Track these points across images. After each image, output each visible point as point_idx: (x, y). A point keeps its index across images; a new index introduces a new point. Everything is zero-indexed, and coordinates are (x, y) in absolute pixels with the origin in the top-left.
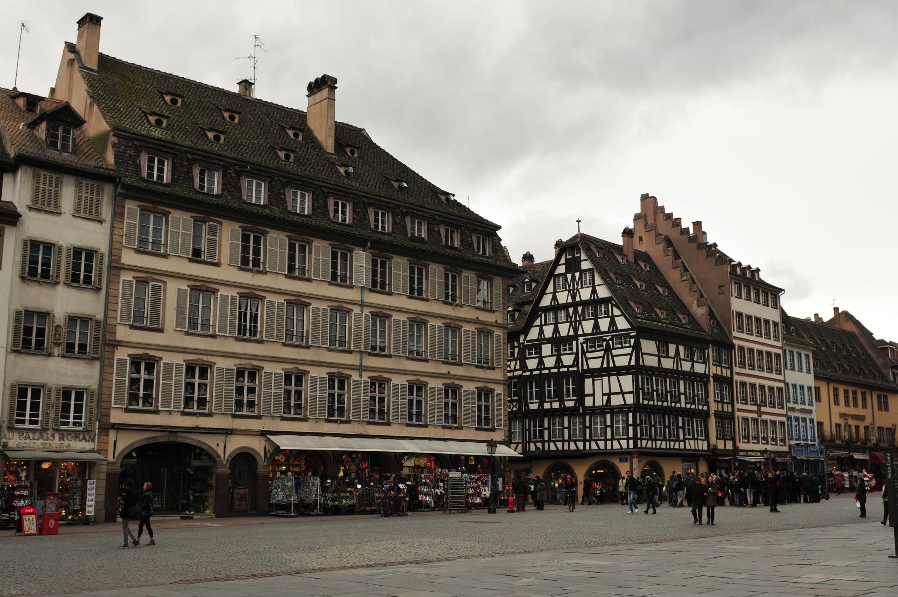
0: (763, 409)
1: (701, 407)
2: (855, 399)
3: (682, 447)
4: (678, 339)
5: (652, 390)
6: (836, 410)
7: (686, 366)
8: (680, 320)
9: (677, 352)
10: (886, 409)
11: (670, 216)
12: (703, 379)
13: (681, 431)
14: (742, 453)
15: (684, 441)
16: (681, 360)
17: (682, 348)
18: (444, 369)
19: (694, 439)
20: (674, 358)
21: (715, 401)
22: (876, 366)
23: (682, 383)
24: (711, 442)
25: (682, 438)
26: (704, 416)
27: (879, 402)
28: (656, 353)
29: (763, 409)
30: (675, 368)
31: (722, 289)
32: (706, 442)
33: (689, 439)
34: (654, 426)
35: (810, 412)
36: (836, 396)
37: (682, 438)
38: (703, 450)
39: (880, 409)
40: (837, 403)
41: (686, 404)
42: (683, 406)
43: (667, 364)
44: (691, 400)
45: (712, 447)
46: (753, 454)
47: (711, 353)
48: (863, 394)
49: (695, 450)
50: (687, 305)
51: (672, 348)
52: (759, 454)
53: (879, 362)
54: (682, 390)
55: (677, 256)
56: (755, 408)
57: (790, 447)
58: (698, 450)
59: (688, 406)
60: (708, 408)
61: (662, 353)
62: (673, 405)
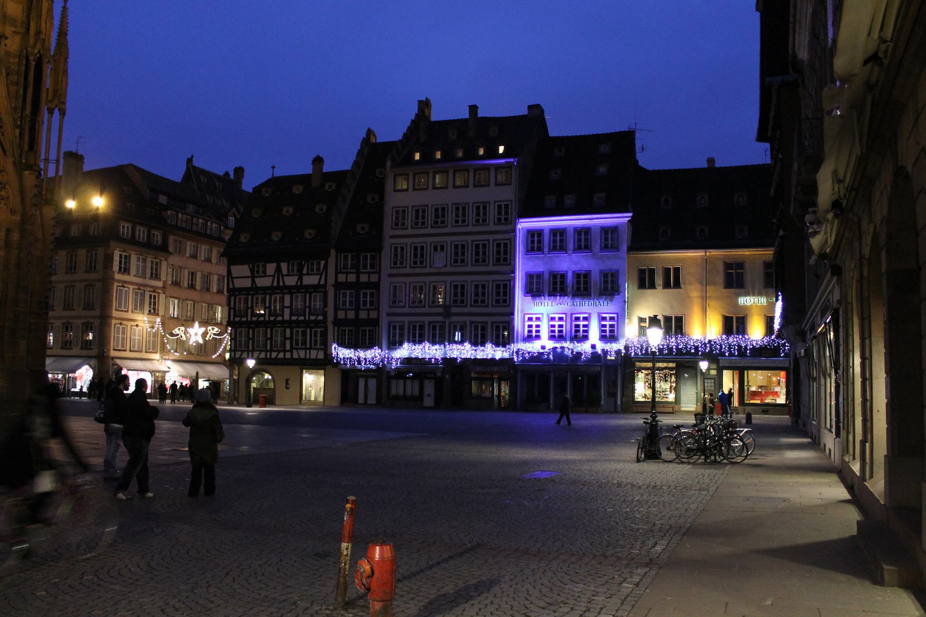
3: (288, 355)
7: (291, 281)
9: (278, 269)
15: (291, 351)
16: (283, 276)
17: (284, 266)
18: (84, 313)
20: (274, 276)
28: (250, 275)
30: (275, 284)
33: (297, 349)
34: (267, 339)
38: (316, 359)
42: (287, 317)
49: (305, 359)
59: (294, 318)
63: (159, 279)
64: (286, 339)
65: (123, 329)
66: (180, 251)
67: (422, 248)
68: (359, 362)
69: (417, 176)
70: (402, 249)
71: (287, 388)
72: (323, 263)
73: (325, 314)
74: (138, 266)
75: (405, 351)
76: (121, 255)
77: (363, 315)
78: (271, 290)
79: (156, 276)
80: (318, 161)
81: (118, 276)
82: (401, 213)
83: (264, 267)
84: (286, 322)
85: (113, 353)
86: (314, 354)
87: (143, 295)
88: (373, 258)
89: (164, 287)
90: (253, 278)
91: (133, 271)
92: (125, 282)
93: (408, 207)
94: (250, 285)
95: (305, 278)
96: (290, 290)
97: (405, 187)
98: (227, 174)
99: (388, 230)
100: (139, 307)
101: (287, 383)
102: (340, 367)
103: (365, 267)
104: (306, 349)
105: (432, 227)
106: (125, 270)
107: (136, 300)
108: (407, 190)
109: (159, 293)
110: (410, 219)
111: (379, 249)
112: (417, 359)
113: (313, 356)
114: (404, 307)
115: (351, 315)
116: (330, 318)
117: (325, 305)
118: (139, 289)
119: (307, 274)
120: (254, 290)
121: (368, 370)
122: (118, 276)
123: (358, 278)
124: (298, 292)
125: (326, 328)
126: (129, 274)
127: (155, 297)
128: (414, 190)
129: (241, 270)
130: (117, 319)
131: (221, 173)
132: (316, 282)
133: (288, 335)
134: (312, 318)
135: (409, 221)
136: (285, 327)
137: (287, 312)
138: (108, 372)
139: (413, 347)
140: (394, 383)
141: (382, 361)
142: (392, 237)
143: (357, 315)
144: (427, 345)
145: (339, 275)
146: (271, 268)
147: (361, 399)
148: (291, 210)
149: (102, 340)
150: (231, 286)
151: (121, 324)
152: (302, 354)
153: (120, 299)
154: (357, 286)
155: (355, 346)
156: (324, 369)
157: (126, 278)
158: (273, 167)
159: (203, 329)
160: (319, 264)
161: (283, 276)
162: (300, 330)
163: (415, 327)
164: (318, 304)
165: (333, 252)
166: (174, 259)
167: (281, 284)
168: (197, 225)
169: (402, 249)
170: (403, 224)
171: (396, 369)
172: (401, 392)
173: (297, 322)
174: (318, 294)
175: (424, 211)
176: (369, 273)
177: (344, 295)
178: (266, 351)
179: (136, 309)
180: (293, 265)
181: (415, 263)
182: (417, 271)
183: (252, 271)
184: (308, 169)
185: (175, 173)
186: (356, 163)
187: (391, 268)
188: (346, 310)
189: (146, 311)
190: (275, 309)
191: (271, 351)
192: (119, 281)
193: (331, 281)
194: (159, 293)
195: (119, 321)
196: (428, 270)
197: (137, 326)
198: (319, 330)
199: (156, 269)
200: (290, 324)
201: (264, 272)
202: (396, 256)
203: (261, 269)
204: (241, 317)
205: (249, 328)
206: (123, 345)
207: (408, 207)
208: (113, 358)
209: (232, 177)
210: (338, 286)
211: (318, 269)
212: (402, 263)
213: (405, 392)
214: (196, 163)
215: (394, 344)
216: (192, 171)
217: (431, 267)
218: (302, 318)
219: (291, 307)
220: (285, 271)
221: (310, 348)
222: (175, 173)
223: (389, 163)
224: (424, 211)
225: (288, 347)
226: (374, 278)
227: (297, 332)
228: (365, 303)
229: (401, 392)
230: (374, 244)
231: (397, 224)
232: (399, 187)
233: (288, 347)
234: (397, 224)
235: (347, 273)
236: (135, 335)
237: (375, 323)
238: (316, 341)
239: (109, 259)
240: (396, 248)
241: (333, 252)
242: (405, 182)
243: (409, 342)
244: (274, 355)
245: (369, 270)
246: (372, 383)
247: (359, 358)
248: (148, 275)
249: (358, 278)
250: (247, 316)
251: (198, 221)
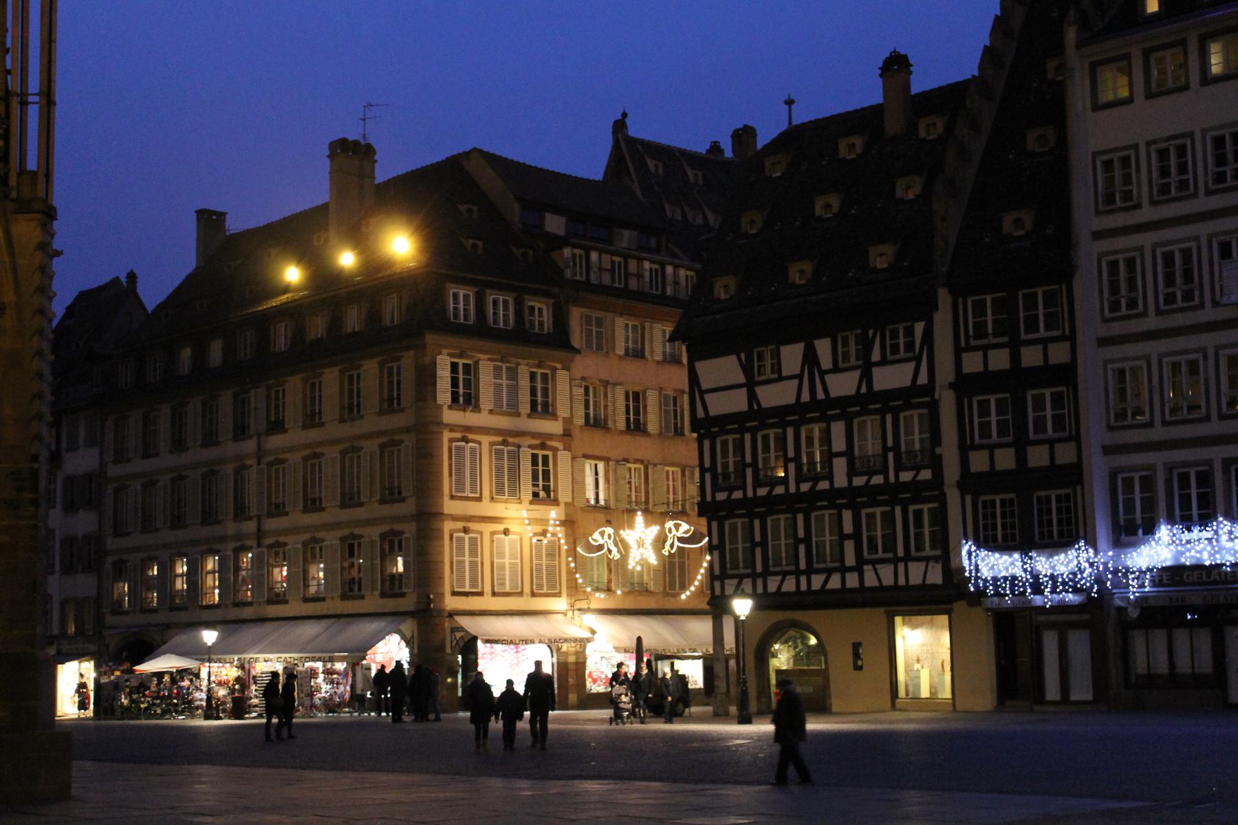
3: (852, 581)
4: (803, 329)
7: (843, 385)
9: (810, 358)
15: (858, 569)
16: (823, 373)
17: (823, 347)
18: (385, 510)
20: (800, 377)
28: (742, 379)
30: (806, 397)
33: (874, 563)
34: (798, 541)
38: (923, 587)
42: (841, 481)
43: (774, 395)
58: (907, 587)
59: (859, 481)
62: (805, 487)
63: (554, 416)
64: (843, 537)
65: (473, 542)
66: (601, 345)
67: (1186, 253)
68: (1037, 588)
69: (1153, 57)
70: (1131, 263)
71: (860, 668)
72: (919, 328)
73: (936, 463)
74: (498, 387)
75: (1161, 549)
76: (454, 367)
77: (1038, 457)
78: (796, 414)
79: (543, 407)
80: (896, 65)
81: (451, 416)
82: (1117, 164)
83: (777, 355)
84: (840, 492)
85: (451, 603)
86: (916, 574)
87: (515, 457)
88: (1050, 299)
89: (567, 434)
90: (750, 386)
91: (486, 398)
92: (468, 429)
93: (1135, 147)
94: (744, 407)
95: (877, 372)
96: (845, 408)
97: (1124, 93)
98: (715, 148)
99: (1085, 215)
100: (507, 486)
101: (857, 656)
102: (988, 603)
103: (1032, 326)
104: (895, 561)
105: (1209, 193)
106: (466, 398)
107: (499, 469)
108: (1129, 101)
109: (555, 450)
110: (1143, 182)
111: (1064, 272)
112: (1198, 567)
113: (915, 580)
114: (1150, 424)
115: (1006, 460)
116: (952, 472)
117: (935, 437)
118: (505, 443)
119: (884, 362)
120: (757, 417)
121: (1061, 608)
122: (451, 416)
123: (1015, 357)
124: (865, 411)
125: (942, 498)
126: (477, 408)
127: (545, 458)
128: (1149, 95)
129: (722, 370)
130: (455, 518)
131: (702, 148)
132: (907, 382)
133: (848, 528)
134: (906, 476)
135: (1142, 187)
136: (840, 508)
137: (840, 465)
138: (443, 648)
139: (1186, 536)
140: (1138, 641)
141: (1099, 580)
142: (1098, 235)
143: (1021, 458)
144: (1225, 526)
145: (964, 356)
146: (792, 356)
147: (1052, 692)
148: (835, 202)
149: (425, 572)
150: (700, 414)
151: (466, 530)
152: (887, 575)
153: (460, 472)
154: (1017, 380)
155: (1023, 543)
156: (948, 612)
157: (470, 418)
158: (789, 102)
159: (655, 530)
160: (910, 332)
161: (823, 373)
162: (878, 511)
163: (1184, 479)
164: (916, 438)
165: (944, 297)
166: (589, 365)
167: (820, 395)
168: (640, 276)
169: (1131, 263)
170: (1127, 196)
171: (1142, 601)
172: (1162, 667)
173: (867, 489)
174: (915, 413)
175: (1181, 150)
176: (1044, 342)
177: (984, 409)
178: (798, 573)
179: (500, 491)
180: (845, 343)
181: (1170, 299)
182: (1178, 320)
183: (747, 369)
184: (871, 93)
185: (588, 160)
186: (990, 55)
187: (1105, 321)
188: (991, 448)
189: (527, 491)
190: (812, 463)
191: (810, 572)
192: (452, 428)
193: (945, 373)
194: (555, 450)
195: (460, 525)
196: (1209, 314)
197: (506, 532)
198: (925, 507)
199: (545, 392)
200: (851, 498)
201: (777, 368)
202: (1115, 290)
203: (768, 363)
204: (731, 490)
205: (751, 516)
206: (474, 583)
207: (1135, 147)
208: (452, 614)
209: (729, 154)
210: (964, 385)
211: (910, 346)
212: (1132, 304)
213: (1172, 664)
214: (636, 129)
215: (1131, 530)
216: (628, 151)
217: (1216, 304)
218: (878, 480)
219: (849, 453)
220: (826, 362)
221: (908, 558)
222: (588, 160)
223: (1071, 35)
224: (1181, 150)
225: (850, 560)
226: (1059, 353)
227: (871, 516)
228: (1040, 424)
229: (1162, 667)
230: (1052, 259)
231: (1110, 199)
232: (1109, 96)
233: (850, 560)
234: (1110, 199)
235: (985, 349)
236: (501, 555)
237: (1073, 475)
238: (919, 537)
239: (426, 377)
240: (1113, 265)
241: (944, 297)
242: (1124, 80)
243: (1171, 521)
244: (817, 581)
245: (1042, 333)
246: (1080, 644)
247: (1036, 577)
248: (525, 408)
249: (1015, 357)
250: (743, 487)
251: (640, 267)
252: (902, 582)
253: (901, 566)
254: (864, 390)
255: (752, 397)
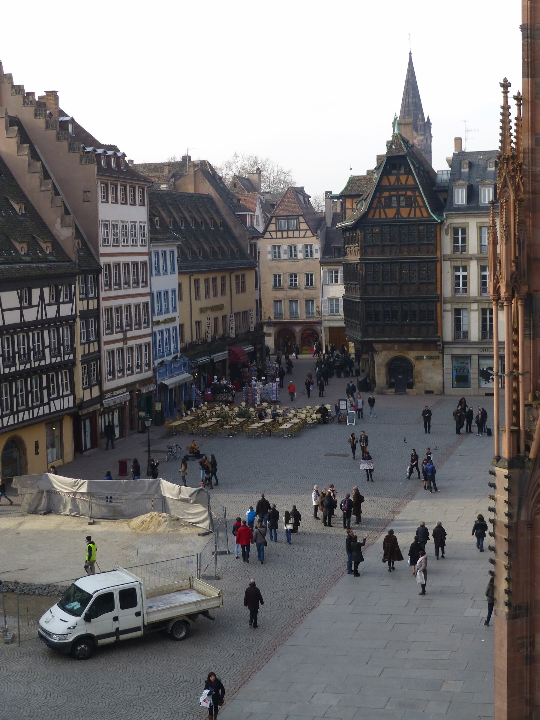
0: (129, 334)
1: (66, 357)
2: (215, 286)
5: (14, 353)
6: (197, 305)
7: (51, 312)
8: (42, 251)
10: (244, 290)
11: (19, 89)
12: (69, 321)
13: (45, 392)
14: (107, 395)
15: (48, 403)
17: (46, 290)
19: (59, 397)
20: (37, 306)
21: (82, 344)
22: (233, 237)
23: (46, 333)
24: (77, 397)
25: (46, 400)
26: (70, 365)
27: (237, 283)
29: (129, 334)
31: (88, 196)
32: (71, 397)
35: (173, 320)
36: (197, 289)
37: (46, 400)
38: (69, 408)
39: (238, 292)
40: (197, 297)
41: (51, 357)
43: (31, 315)
44: (56, 352)
45: (78, 401)
46: (119, 392)
47: (77, 286)
48: (223, 278)
50: (47, 223)
51: (36, 293)
52: (124, 390)
53: (237, 232)
54: (47, 343)
55: (34, 155)
56: (120, 336)
57: (155, 371)
60: (75, 356)
61: (25, 302)
62: (37, 364)
117: (73, 340)
167: (44, 317)
252: (62, 408)
253: (61, 399)
254: (57, 316)
255: (22, 315)
